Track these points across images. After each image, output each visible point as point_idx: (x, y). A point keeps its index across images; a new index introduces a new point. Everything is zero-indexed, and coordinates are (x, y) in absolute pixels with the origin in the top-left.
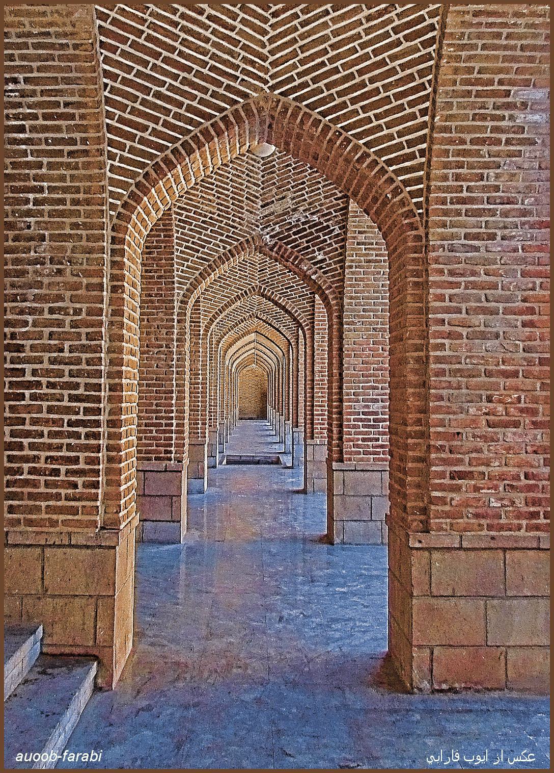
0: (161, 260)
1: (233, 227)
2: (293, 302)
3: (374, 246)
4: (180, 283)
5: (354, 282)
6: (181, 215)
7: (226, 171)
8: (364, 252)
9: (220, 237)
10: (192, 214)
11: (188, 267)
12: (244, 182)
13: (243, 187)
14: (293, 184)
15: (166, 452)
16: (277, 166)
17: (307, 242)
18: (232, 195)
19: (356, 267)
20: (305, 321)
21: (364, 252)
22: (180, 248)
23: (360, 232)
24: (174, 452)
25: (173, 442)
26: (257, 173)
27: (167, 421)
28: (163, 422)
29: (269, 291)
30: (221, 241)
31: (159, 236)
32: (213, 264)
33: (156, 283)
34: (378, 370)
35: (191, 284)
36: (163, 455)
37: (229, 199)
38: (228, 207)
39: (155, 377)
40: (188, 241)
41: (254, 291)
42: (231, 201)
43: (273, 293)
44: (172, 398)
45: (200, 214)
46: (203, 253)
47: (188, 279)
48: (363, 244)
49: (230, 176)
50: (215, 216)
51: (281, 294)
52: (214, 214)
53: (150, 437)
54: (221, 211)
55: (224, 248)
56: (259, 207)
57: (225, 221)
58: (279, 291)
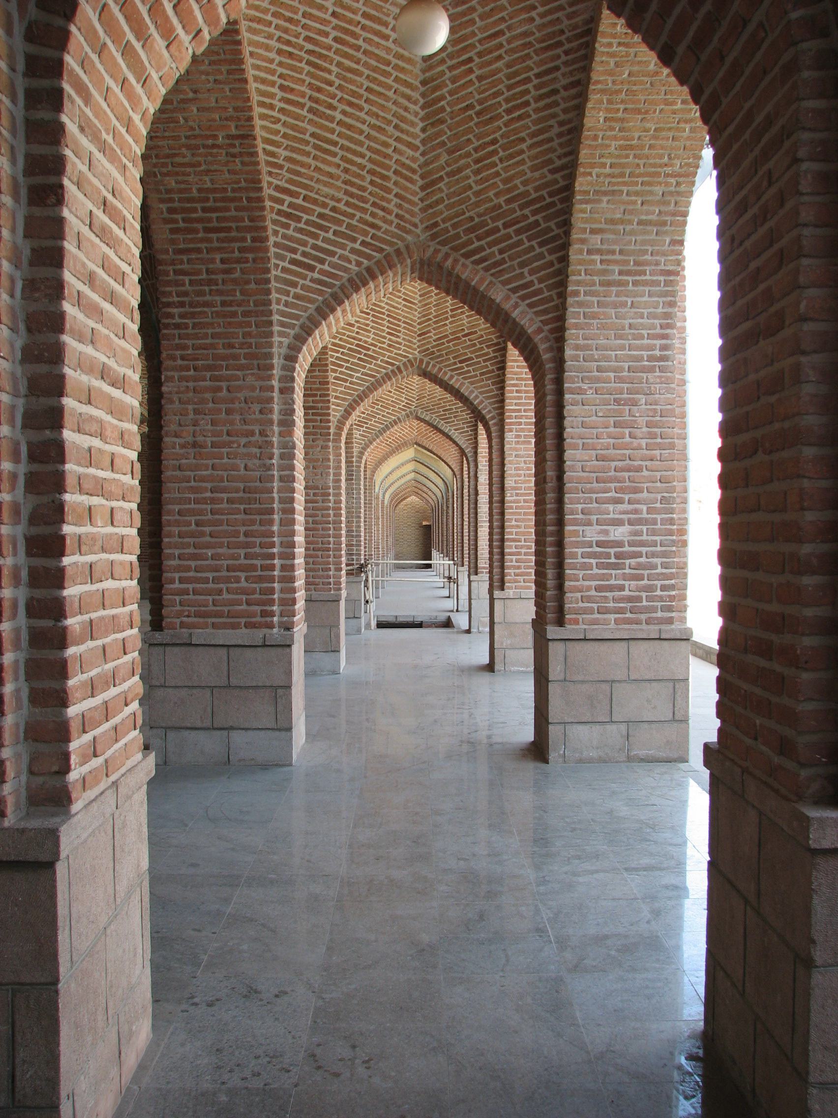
0: (248, 282)
1: (373, 226)
2: (472, 383)
3: (617, 257)
4: (283, 324)
5: (582, 320)
6: (281, 202)
7: (358, 119)
8: (599, 266)
9: (351, 245)
10: (300, 201)
11: (297, 297)
12: (390, 141)
13: (390, 151)
14: (477, 144)
15: (264, 614)
16: (448, 109)
17: (501, 252)
18: (369, 166)
19: (586, 294)
20: (489, 412)
21: (599, 266)
22: (282, 264)
23: (593, 231)
24: (277, 613)
25: (276, 596)
26: (413, 124)
27: (263, 562)
28: (258, 562)
29: (434, 366)
30: (353, 251)
31: (244, 239)
32: (339, 291)
33: (240, 325)
34: (622, 470)
36: (258, 619)
37: (364, 173)
38: (363, 189)
39: (242, 485)
40: (294, 251)
41: (412, 365)
42: (369, 178)
43: (440, 369)
44: (271, 522)
45: (315, 202)
46: (322, 272)
47: (297, 317)
48: (599, 252)
49: (365, 128)
50: (341, 206)
51: (452, 370)
52: (339, 201)
53: (237, 588)
54: (352, 195)
55: (359, 264)
56: (418, 190)
57: (359, 215)
58: (449, 365)
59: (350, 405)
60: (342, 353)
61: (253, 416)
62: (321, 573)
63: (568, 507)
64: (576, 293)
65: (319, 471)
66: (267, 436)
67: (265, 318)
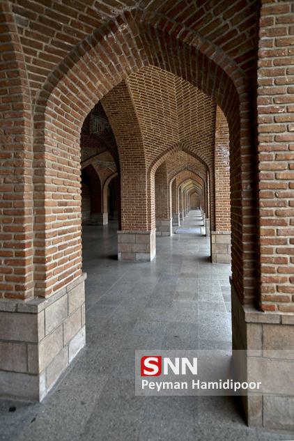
35: (49, 80)
47: (46, 73)
55: (89, 30)
61: (10, 143)
63: (263, 209)
64: (269, 22)
66: (19, 157)
67: (13, 70)
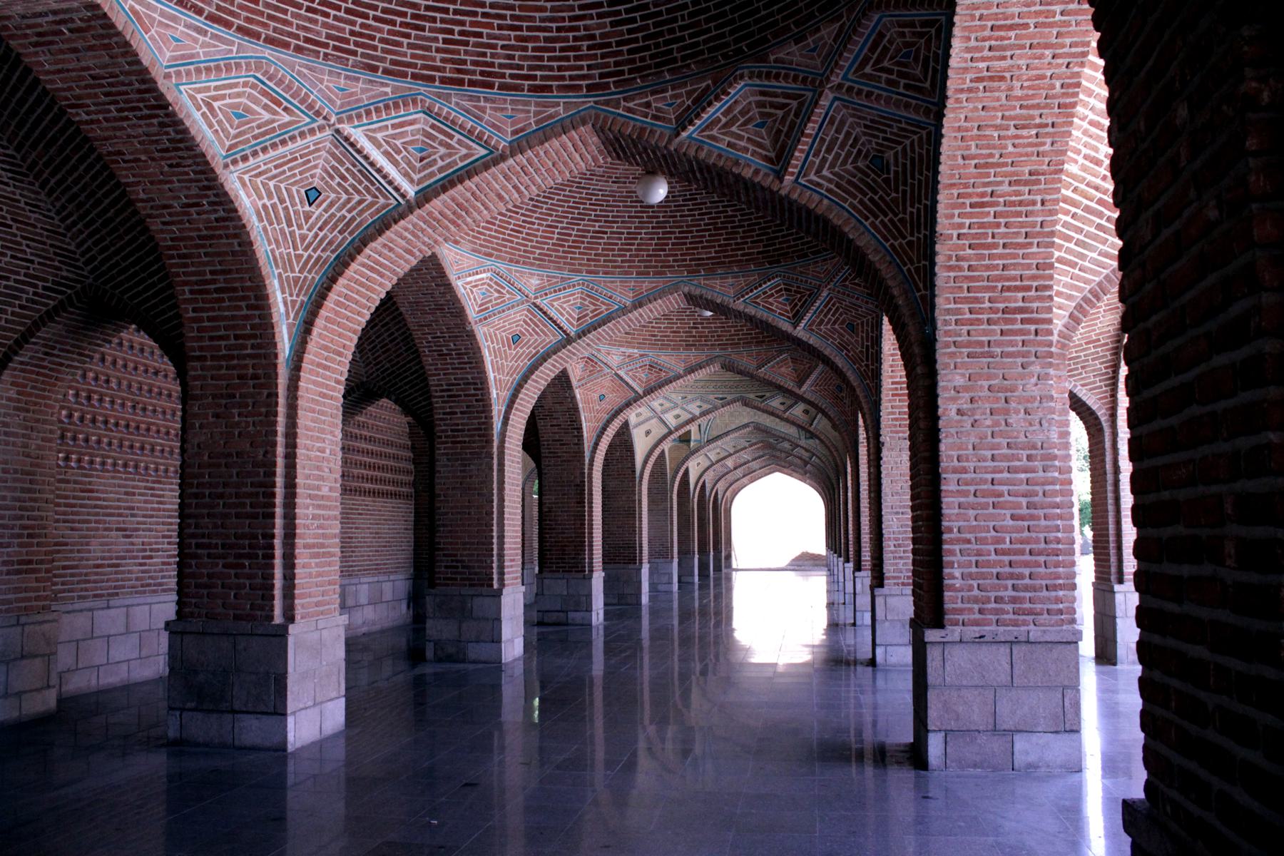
59: (1079, 307)
60: (1074, 216)
62: (1045, 593)
65: (1035, 418)
